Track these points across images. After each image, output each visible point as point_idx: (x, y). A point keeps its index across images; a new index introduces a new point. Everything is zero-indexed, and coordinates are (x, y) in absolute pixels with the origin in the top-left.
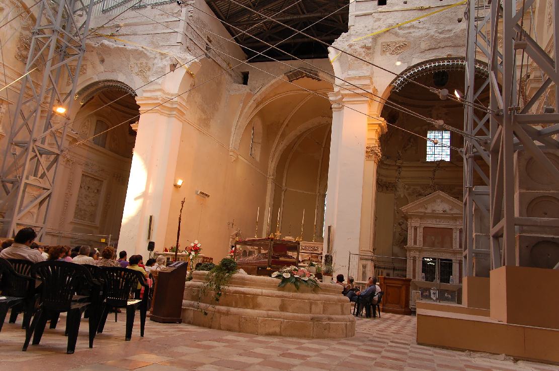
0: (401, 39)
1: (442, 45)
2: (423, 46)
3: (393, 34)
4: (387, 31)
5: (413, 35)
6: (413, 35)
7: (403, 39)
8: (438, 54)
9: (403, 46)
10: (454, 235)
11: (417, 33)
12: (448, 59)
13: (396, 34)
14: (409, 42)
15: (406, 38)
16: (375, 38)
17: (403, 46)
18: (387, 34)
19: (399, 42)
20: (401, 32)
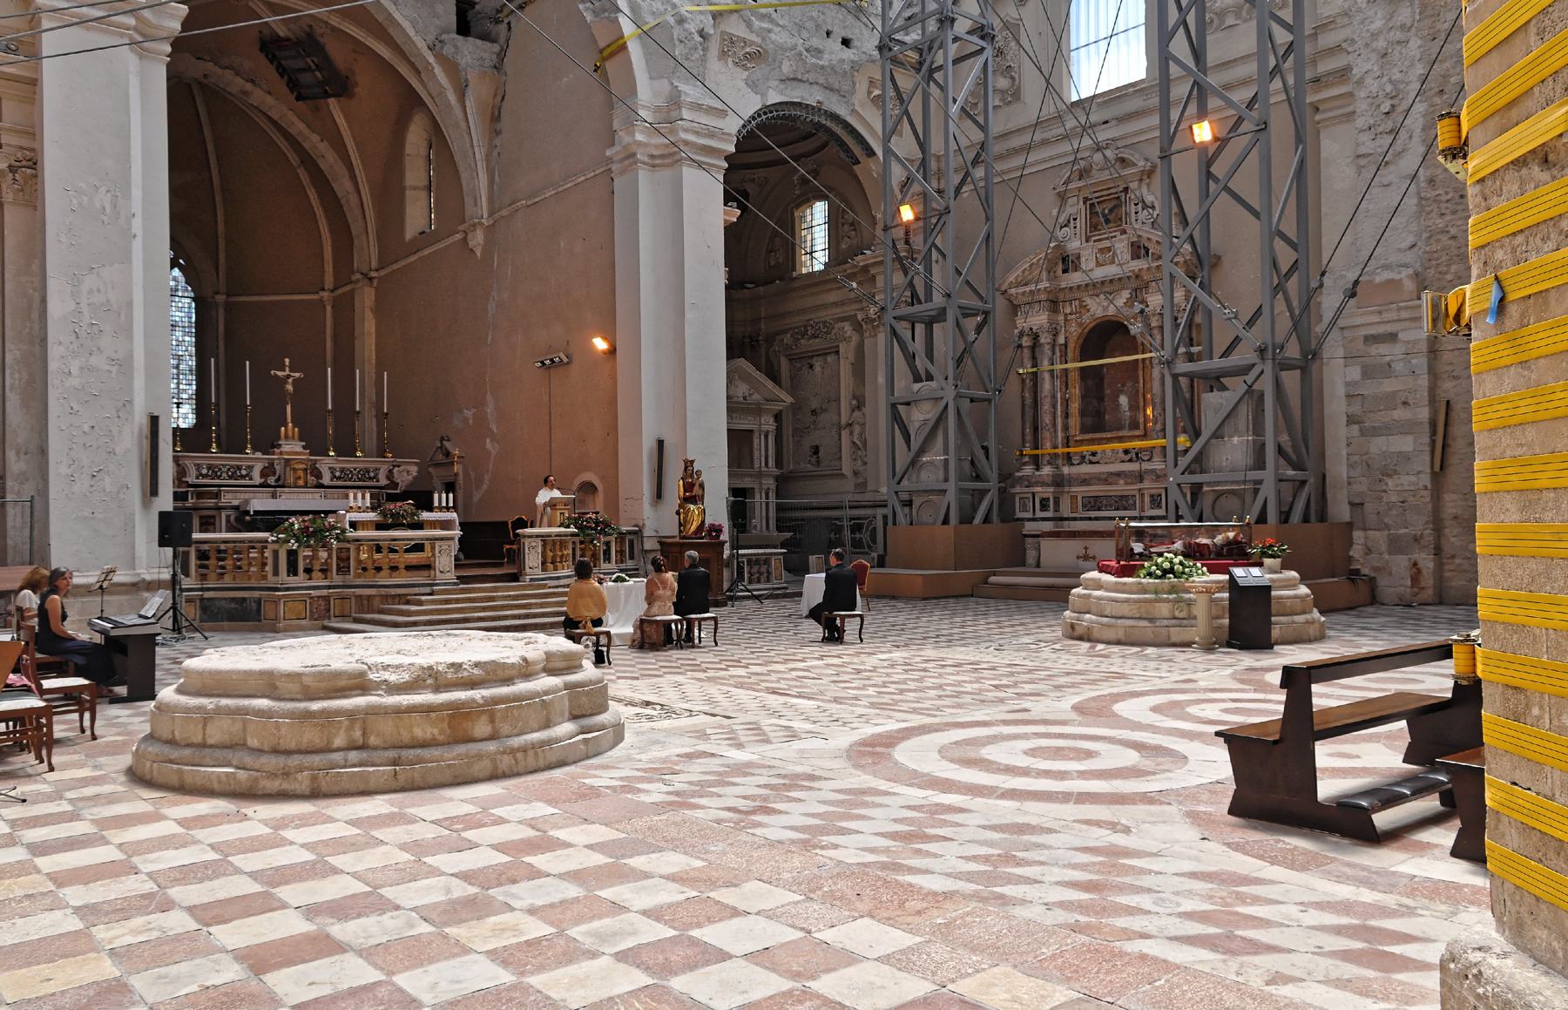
0: (753, 37)
1: (811, 77)
2: (786, 68)
3: (745, 21)
4: (736, 11)
5: (773, 36)
6: (773, 36)
7: (758, 40)
8: (807, 96)
9: (757, 56)
10: (756, 441)
11: (780, 37)
12: (817, 110)
13: (749, 25)
14: (766, 51)
15: (764, 39)
16: (716, 16)
17: (757, 56)
18: (735, 17)
19: (753, 43)
20: (757, 24)
